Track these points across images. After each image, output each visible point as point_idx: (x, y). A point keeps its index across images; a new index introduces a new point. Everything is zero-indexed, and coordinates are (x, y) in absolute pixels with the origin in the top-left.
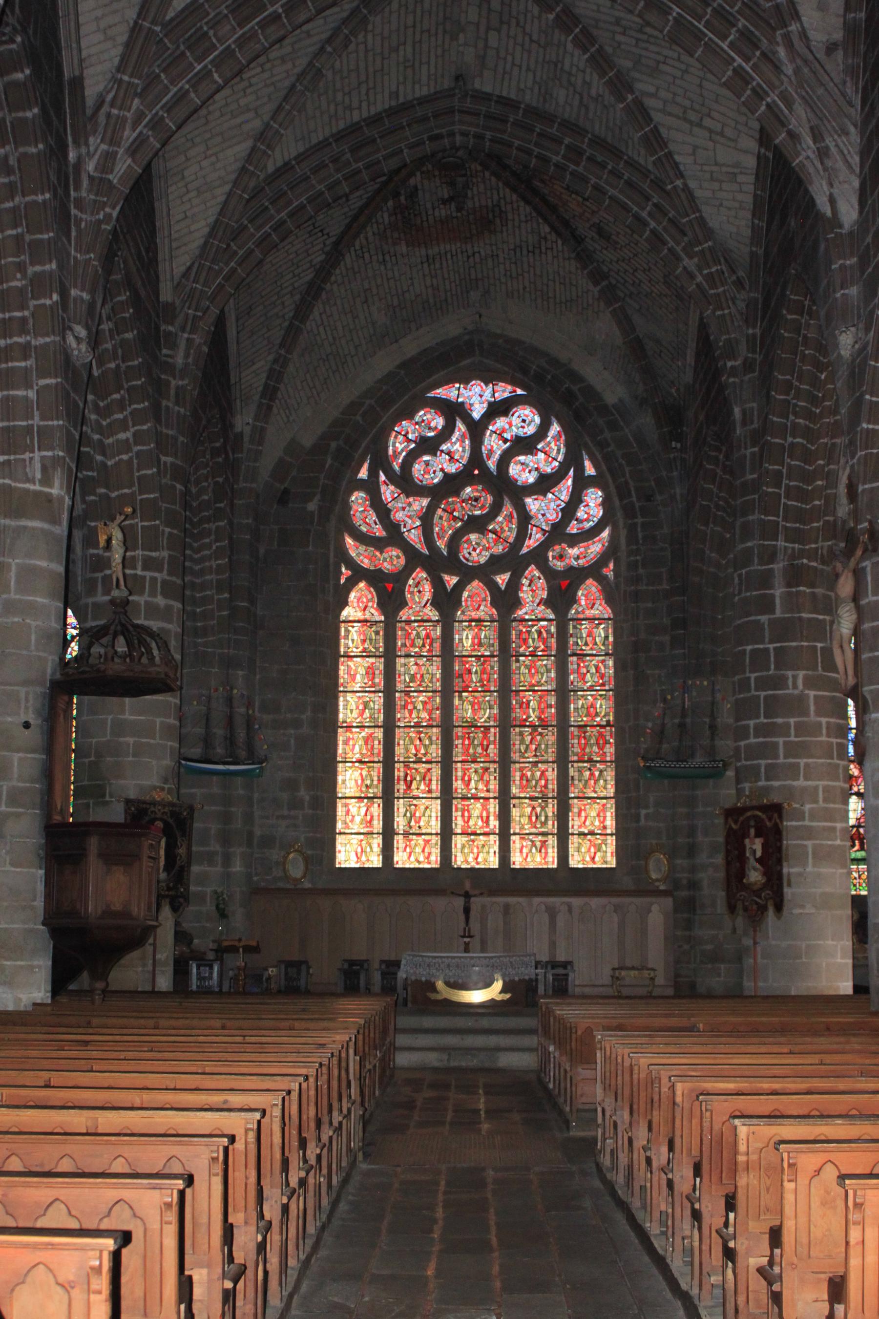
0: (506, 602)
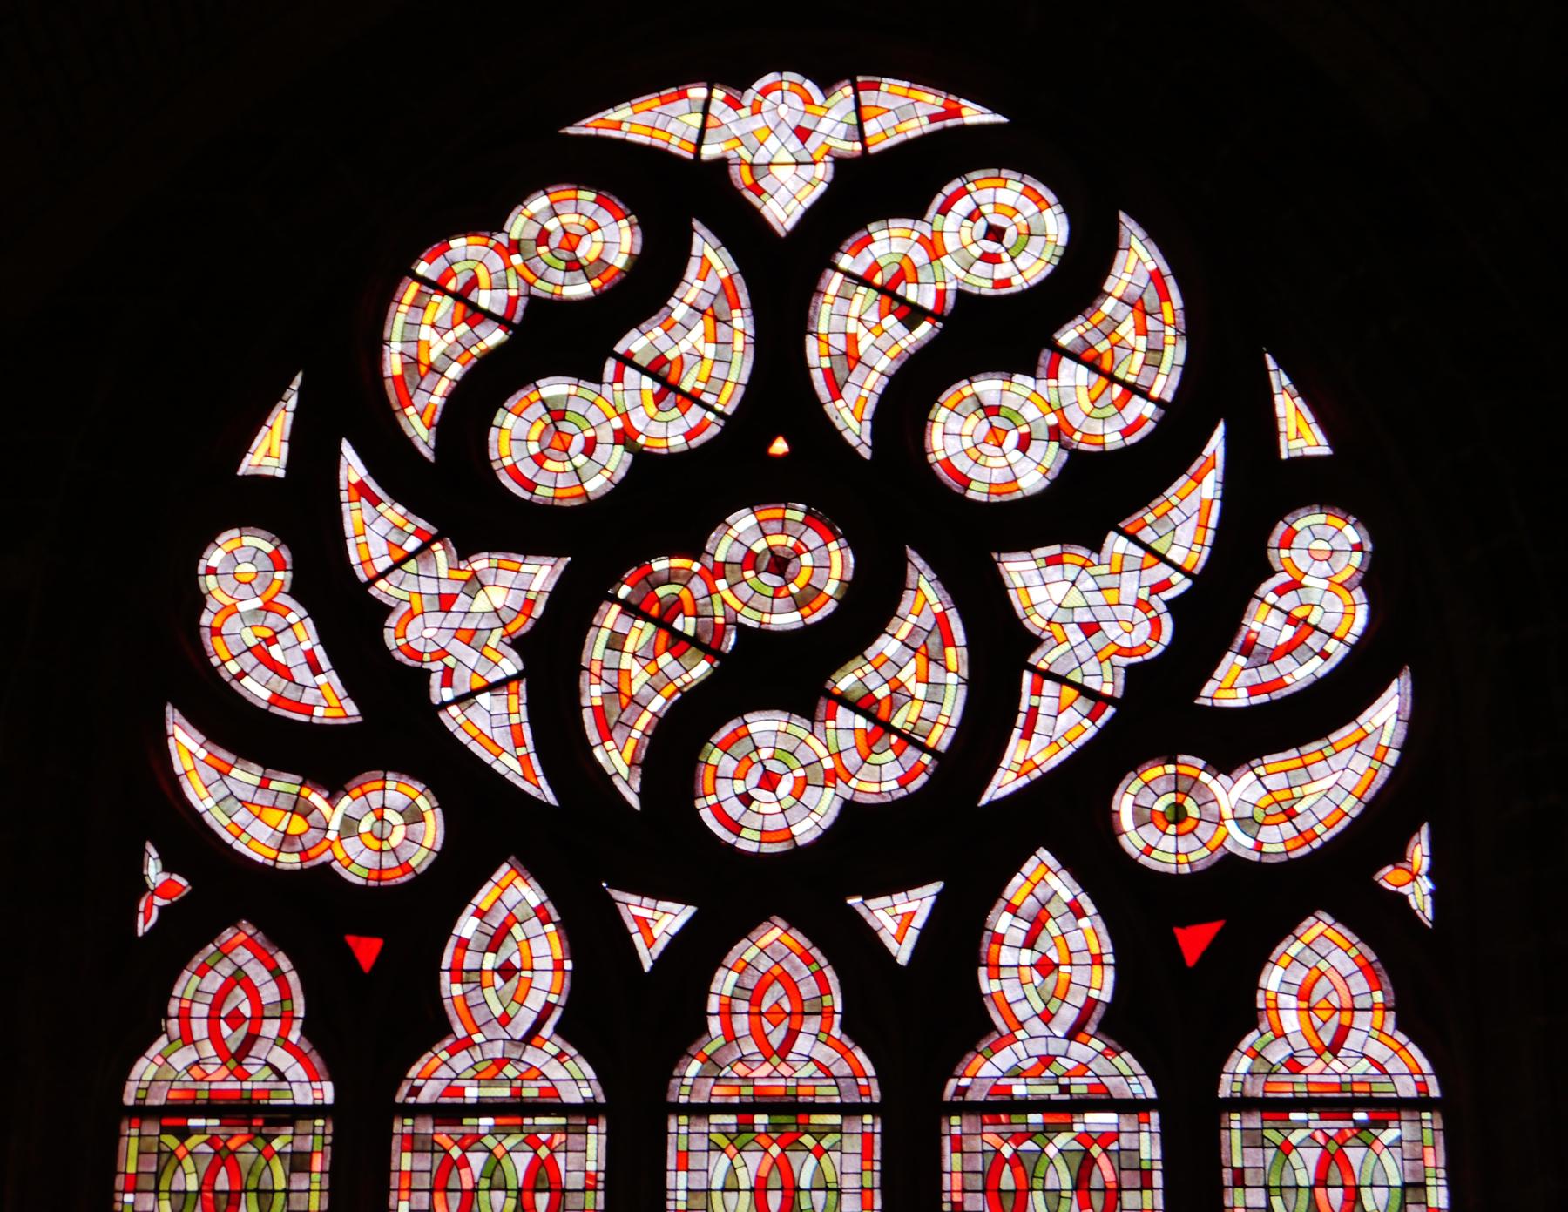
0: (920, 1021)
